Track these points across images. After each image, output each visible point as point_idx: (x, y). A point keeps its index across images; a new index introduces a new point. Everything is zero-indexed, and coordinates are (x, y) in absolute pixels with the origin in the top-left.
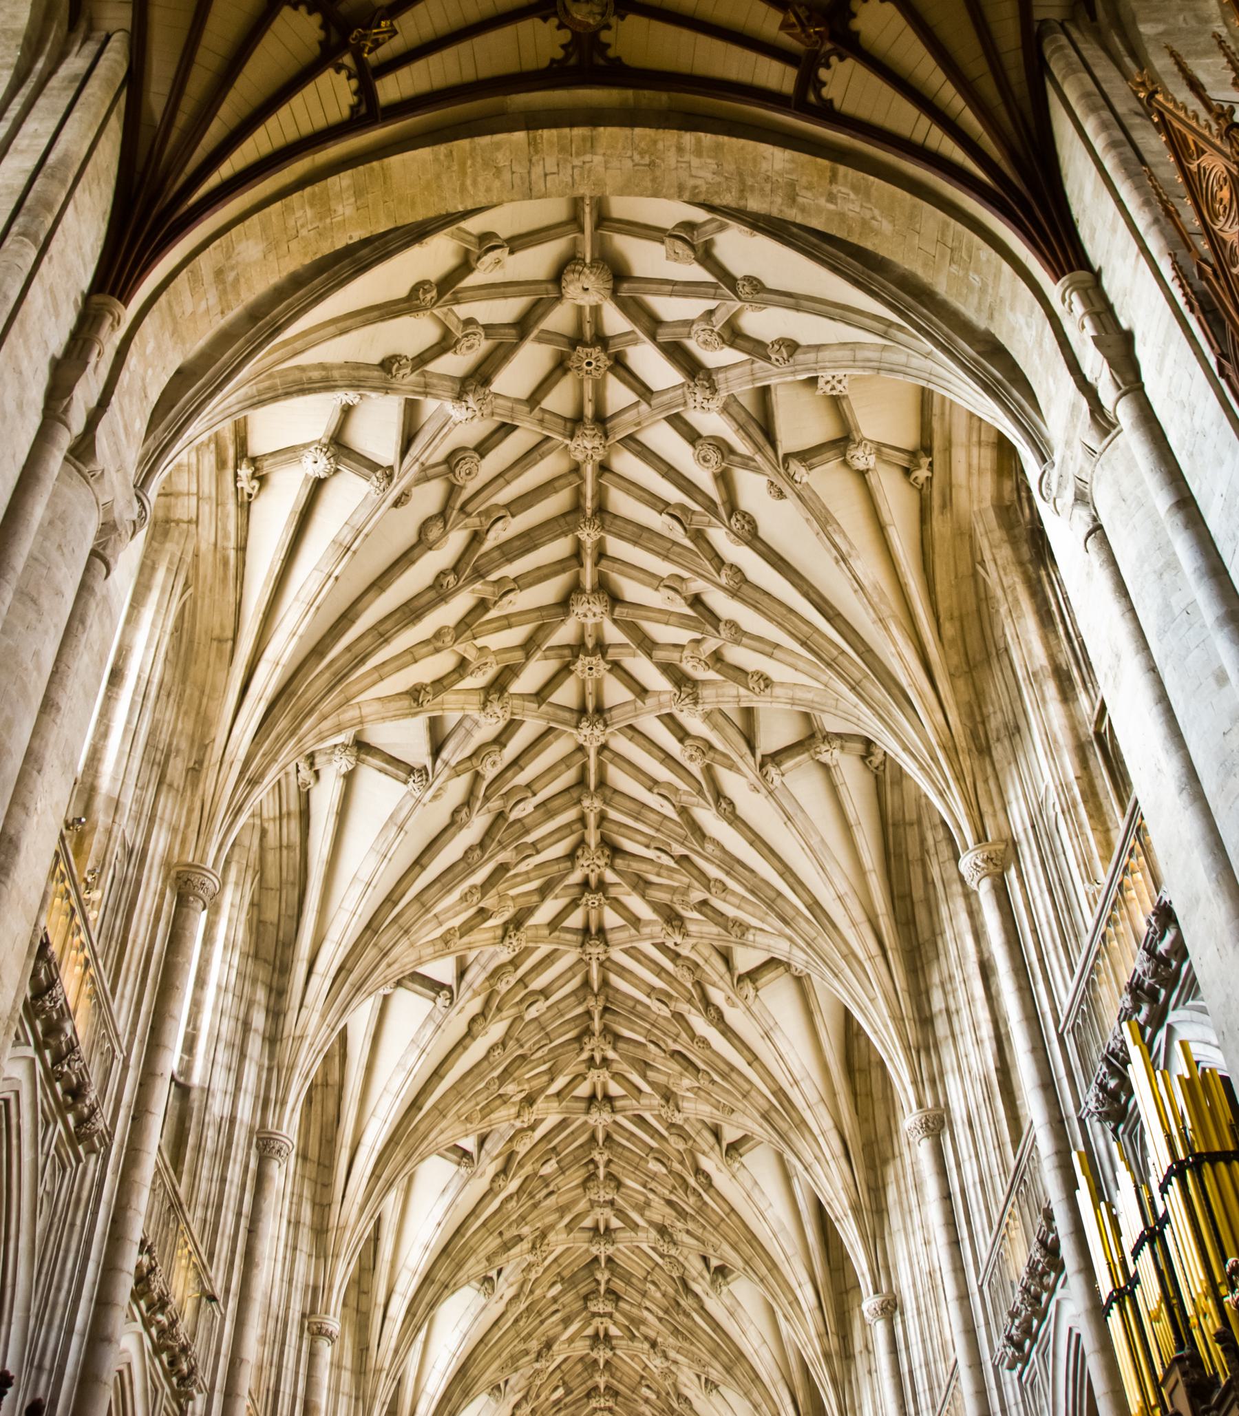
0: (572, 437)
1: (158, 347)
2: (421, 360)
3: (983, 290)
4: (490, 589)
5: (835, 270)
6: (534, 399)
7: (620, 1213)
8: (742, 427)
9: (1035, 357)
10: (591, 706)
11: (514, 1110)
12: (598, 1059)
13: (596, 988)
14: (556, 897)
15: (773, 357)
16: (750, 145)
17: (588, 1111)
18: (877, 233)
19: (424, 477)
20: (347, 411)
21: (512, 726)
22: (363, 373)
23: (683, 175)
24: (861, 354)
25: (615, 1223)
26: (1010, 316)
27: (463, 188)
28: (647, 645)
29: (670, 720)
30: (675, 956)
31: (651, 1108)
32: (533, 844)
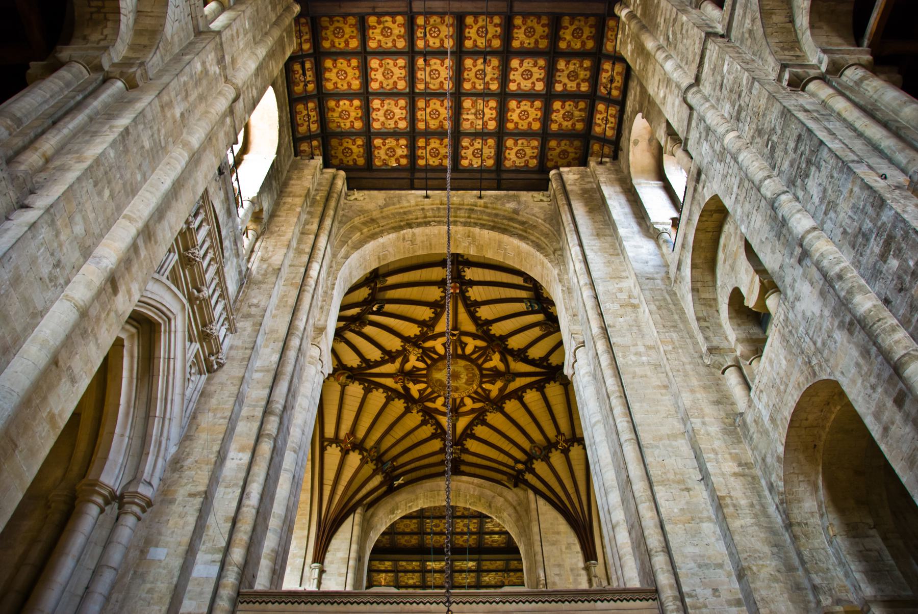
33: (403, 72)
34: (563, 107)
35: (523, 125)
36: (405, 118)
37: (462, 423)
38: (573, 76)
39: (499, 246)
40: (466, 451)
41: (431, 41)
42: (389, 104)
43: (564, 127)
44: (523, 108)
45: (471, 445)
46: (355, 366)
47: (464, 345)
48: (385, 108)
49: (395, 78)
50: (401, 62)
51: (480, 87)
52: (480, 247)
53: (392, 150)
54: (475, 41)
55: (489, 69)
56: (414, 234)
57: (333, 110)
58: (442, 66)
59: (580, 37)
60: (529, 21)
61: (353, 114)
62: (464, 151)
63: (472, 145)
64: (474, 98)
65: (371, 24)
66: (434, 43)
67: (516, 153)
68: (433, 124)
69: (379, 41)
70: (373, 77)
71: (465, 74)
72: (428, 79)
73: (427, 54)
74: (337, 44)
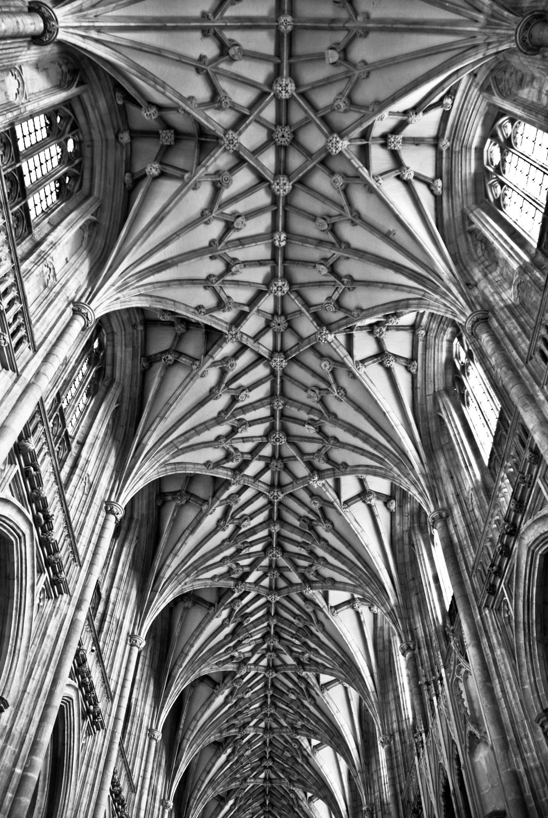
4: (236, 422)
7: (276, 721)
10: (276, 484)
11: (235, 666)
12: (271, 648)
13: (273, 614)
14: (258, 570)
17: (266, 672)
19: (214, 364)
21: (245, 488)
25: (275, 725)
28: (302, 453)
29: (307, 489)
30: (306, 599)
31: (291, 669)
32: (250, 542)
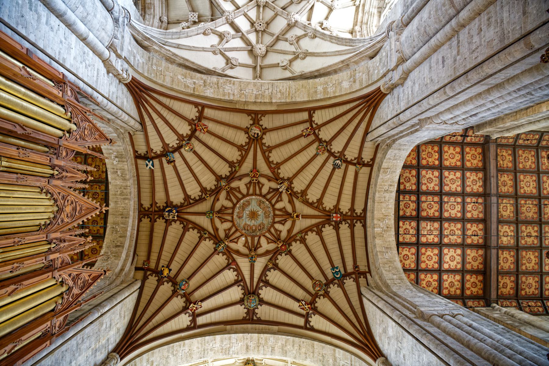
0: (267, 2)
1: (374, 70)
2: (305, 35)
3: (152, 65)
5: (193, 63)
6: (276, 15)
8: (219, 6)
9: (135, 52)
15: (210, 31)
16: (216, 97)
18: (182, 75)
20: (327, 18)
22: (321, 37)
23: (233, 88)
24: (186, 35)
26: (144, 60)
27: (289, 88)
33: (454, 190)
34: (434, 280)
35: (423, 258)
36: (428, 189)
37: (204, 221)
38: (452, 284)
39: (387, 248)
40: (168, 223)
41: (470, 206)
42: (436, 181)
43: (422, 282)
44: (434, 257)
45: (175, 229)
46: (264, 141)
47: (283, 223)
48: (434, 179)
49: (450, 185)
50: (459, 189)
51: (446, 232)
52: (381, 235)
53: (409, 181)
54: (470, 229)
55: (455, 237)
56: (391, 192)
57: (432, 149)
58: (457, 211)
59: (472, 286)
60: (480, 258)
61: (430, 160)
62: (408, 223)
63: (412, 228)
64: (439, 229)
65: (478, 174)
66: (469, 207)
67: (407, 255)
68: (424, 206)
69: (470, 178)
70: (451, 173)
71: (453, 224)
72: (450, 203)
73: (464, 203)
74: (468, 155)
